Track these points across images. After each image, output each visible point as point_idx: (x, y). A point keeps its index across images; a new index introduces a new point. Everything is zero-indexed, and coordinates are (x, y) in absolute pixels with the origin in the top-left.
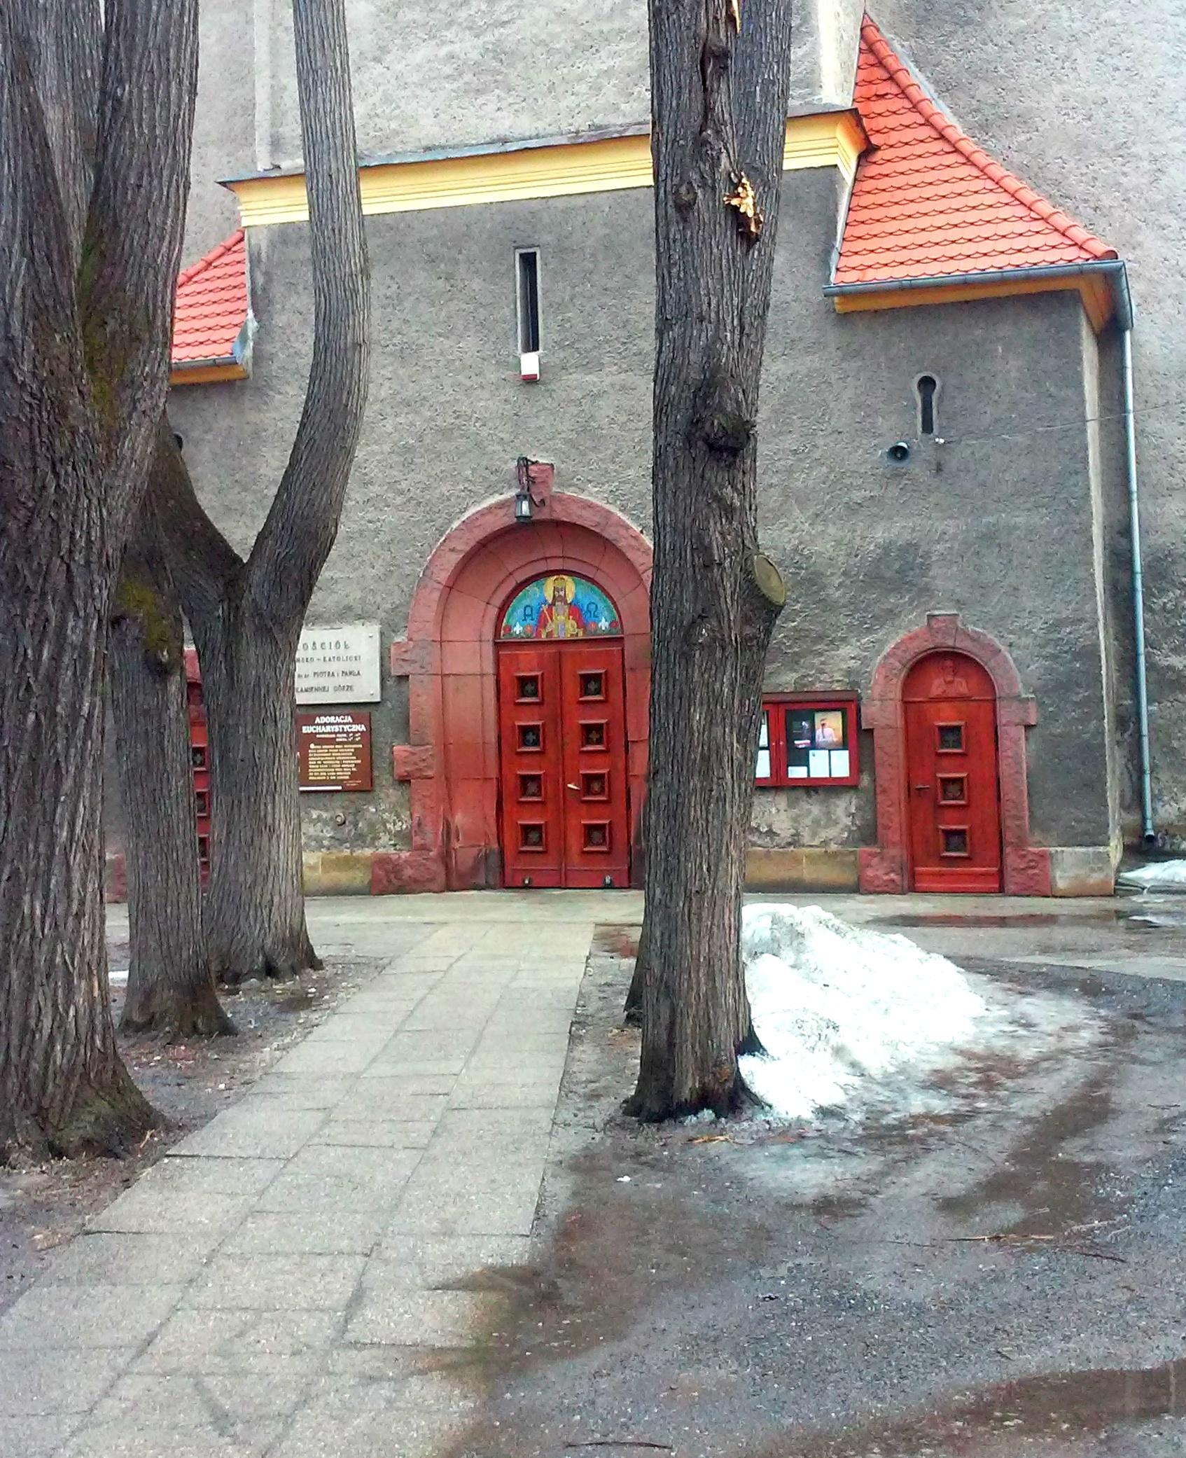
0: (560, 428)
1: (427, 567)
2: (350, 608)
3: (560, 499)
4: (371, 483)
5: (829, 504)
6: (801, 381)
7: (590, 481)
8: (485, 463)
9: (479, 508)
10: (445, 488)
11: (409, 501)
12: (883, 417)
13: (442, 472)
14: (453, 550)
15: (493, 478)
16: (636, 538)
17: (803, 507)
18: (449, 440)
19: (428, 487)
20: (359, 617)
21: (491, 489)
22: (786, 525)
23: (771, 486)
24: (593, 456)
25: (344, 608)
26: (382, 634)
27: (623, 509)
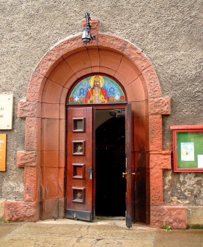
0: (103, 6)
1: (37, 68)
3: (102, 36)
4: (13, 31)
7: (117, 29)
8: (67, 21)
9: (63, 41)
10: (47, 33)
11: (30, 38)
14: (50, 60)
15: (70, 28)
16: (140, 54)
18: (50, 12)
19: (39, 32)
20: (4, 90)
21: (69, 32)
24: (119, 18)
26: (14, 98)
27: (133, 41)
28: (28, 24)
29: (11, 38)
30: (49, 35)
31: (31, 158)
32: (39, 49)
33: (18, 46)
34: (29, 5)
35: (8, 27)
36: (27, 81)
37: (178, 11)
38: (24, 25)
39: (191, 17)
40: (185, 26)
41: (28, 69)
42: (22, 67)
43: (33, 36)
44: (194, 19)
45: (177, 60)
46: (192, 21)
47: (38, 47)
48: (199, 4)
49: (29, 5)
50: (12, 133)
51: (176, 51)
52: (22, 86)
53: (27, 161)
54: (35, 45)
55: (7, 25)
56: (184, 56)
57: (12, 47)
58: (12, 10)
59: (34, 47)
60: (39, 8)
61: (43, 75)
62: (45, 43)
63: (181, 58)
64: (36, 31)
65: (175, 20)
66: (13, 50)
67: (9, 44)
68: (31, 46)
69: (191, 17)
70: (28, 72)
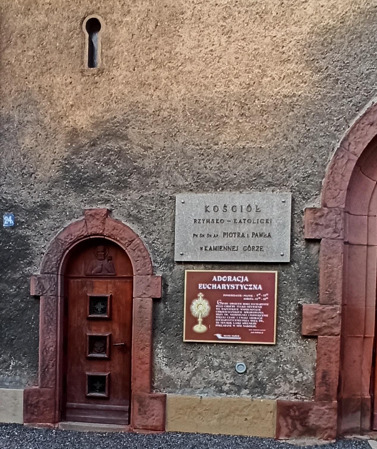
2: (260, 176)
10: (364, 68)
11: (326, 78)
13: (362, 52)
19: (347, 66)
20: (270, 184)
25: (254, 175)
28: (320, 47)
29: (282, 76)
30: (368, 72)
31: (333, 318)
32: (346, 102)
33: (300, 93)
34: (322, 6)
35: (274, 52)
36: (320, 166)
38: (311, 48)
41: (322, 141)
42: (309, 137)
43: (334, 74)
47: (344, 98)
49: (322, 6)
50: (286, 269)
52: (308, 176)
53: (324, 324)
54: (337, 94)
55: (273, 47)
57: (285, 96)
58: (282, 15)
59: (335, 96)
60: (346, 12)
61: (355, 155)
62: (360, 90)
64: (339, 64)
66: (288, 101)
67: (278, 89)
68: (328, 95)
70: (323, 149)
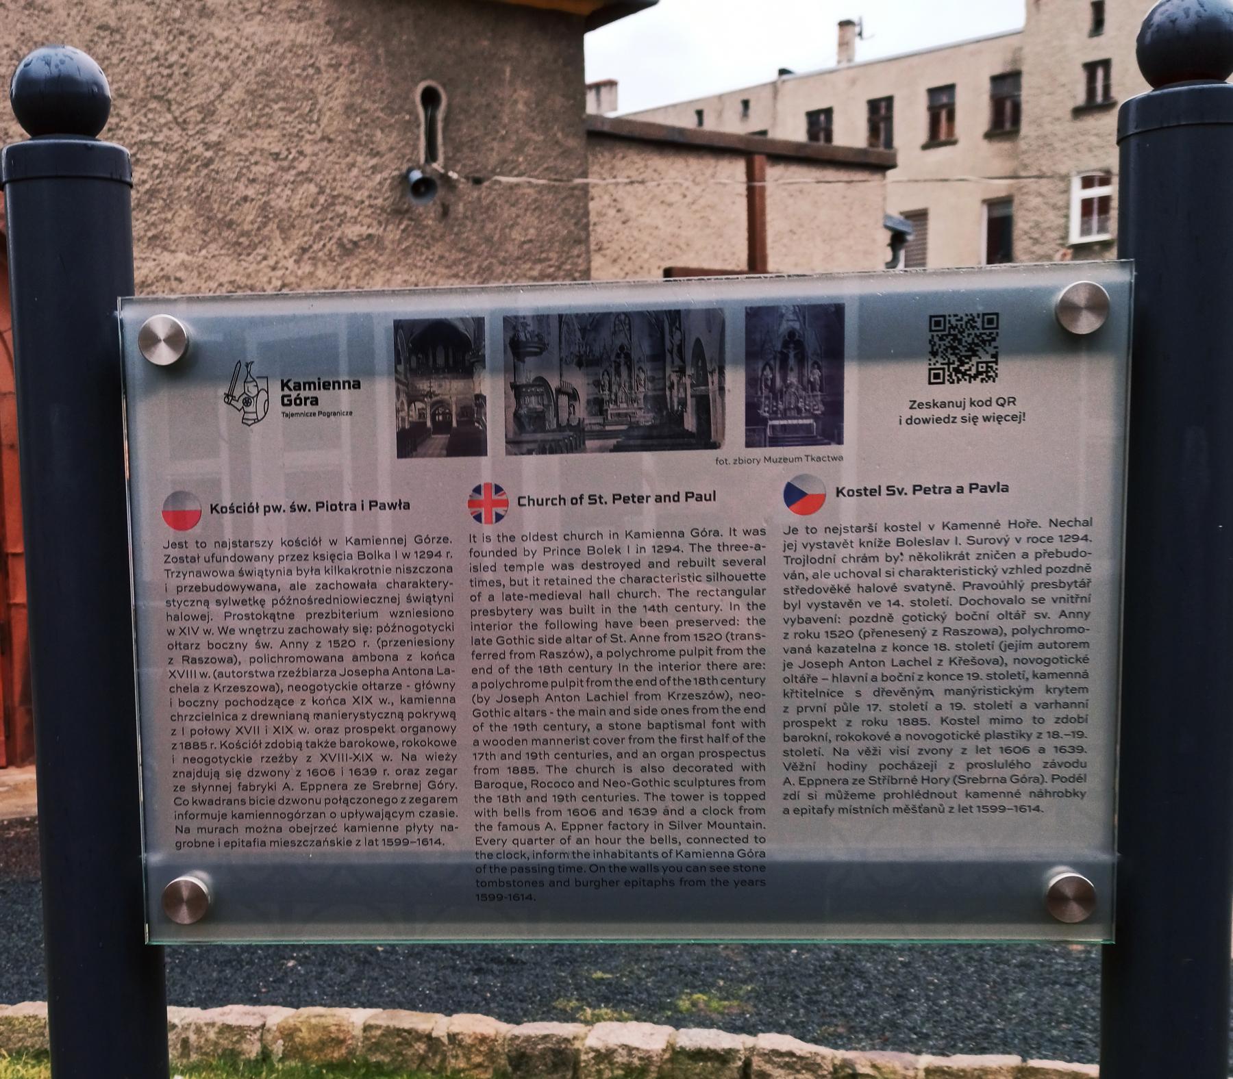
5: (319, 236)
6: (282, 57)
12: (382, 131)
17: (285, 232)
22: (265, 258)
23: (245, 199)
37: (169, 117)
39: (208, 146)
40: (190, 173)
44: (216, 153)
45: (168, 278)
46: (211, 161)
48: (231, 106)
51: (165, 248)
56: (186, 268)
63: (178, 275)
65: (162, 146)
69: (208, 146)
